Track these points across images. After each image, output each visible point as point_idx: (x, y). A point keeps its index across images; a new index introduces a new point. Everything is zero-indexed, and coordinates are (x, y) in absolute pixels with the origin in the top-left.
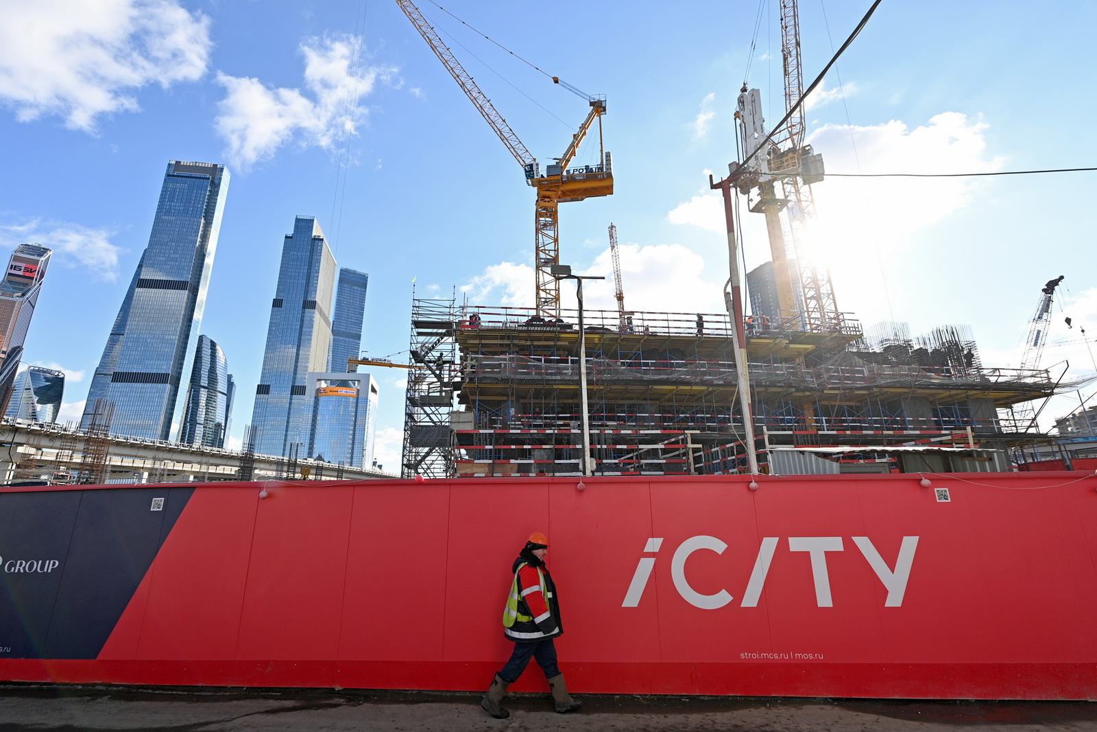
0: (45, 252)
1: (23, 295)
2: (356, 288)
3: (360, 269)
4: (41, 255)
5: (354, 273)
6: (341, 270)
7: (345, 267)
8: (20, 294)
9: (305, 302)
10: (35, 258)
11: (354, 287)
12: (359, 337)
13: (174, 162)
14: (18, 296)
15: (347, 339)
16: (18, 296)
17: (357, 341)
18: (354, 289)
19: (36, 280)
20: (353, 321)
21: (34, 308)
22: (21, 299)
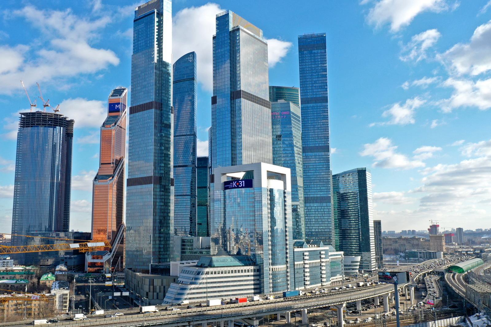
0: (123, 92)
1: (115, 124)
2: (316, 51)
3: (316, 31)
4: (120, 95)
5: (312, 37)
6: (299, 39)
7: (302, 33)
8: (114, 124)
9: (232, 93)
10: (118, 97)
11: (313, 51)
12: (325, 100)
13: (137, 9)
14: (113, 126)
15: (315, 105)
16: (113, 126)
17: (324, 104)
18: (315, 53)
19: (121, 112)
20: (317, 85)
21: (125, 130)
22: (113, 128)
